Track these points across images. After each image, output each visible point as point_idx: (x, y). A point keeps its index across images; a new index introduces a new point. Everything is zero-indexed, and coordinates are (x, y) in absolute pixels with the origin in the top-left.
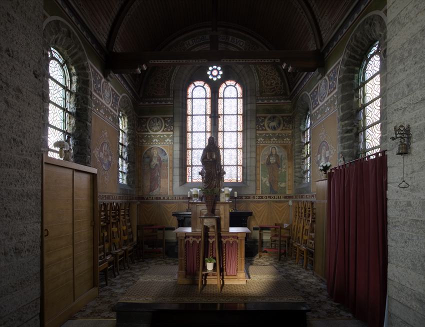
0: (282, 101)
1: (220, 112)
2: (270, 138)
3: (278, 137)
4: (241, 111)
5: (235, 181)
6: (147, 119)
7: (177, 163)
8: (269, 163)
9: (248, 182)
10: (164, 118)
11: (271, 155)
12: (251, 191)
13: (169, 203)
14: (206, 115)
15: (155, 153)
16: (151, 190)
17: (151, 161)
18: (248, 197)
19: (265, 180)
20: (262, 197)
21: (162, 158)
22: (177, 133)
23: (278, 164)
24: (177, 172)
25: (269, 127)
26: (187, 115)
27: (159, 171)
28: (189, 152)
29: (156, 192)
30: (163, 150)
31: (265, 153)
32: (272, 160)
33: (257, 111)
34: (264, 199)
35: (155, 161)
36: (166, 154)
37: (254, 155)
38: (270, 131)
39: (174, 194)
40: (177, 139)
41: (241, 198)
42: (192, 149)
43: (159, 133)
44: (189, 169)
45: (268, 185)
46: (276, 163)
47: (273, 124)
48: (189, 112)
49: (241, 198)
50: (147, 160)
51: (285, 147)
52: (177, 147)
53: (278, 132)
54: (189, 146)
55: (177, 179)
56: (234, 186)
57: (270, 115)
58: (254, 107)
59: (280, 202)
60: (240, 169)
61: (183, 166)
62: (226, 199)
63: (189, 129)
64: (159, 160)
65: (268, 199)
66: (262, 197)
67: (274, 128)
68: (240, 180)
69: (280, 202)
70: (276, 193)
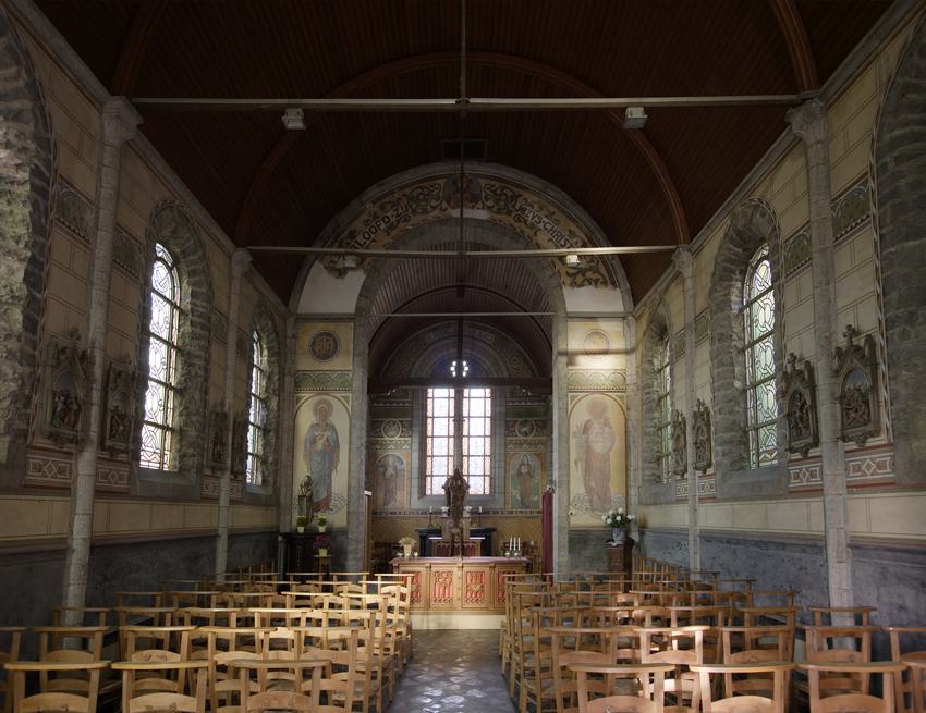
0: (536, 403)
1: (465, 414)
2: (521, 444)
3: (530, 444)
4: (489, 414)
5: (481, 493)
6: (382, 422)
7: (415, 473)
8: (520, 474)
9: (496, 496)
10: (401, 422)
11: (523, 464)
12: (499, 505)
13: (406, 519)
14: (449, 417)
15: (391, 461)
16: (385, 504)
17: (386, 470)
18: (496, 512)
19: (515, 493)
20: (512, 513)
21: (399, 466)
22: (416, 439)
23: (530, 475)
24: (415, 483)
25: (520, 432)
26: (426, 417)
27: (395, 482)
28: (429, 460)
29: (390, 507)
30: (399, 458)
31: (514, 463)
32: (524, 470)
33: (507, 414)
34: (515, 514)
35: (390, 471)
36: (402, 463)
37: (503, 464)
38: (521, 437)
39: (413, 507)
40: (416, 446)
41: (488, 513)
42: (432, 456)
43: (396, 438)
44: (429, 479)
45: (519, 498)
46: (529, 473)
47: (525, 429)
48: (429, 414)
49: (488, 513)
50: (381, 469)
51: (538, 455)
52: (416, 455)
53: (529, 438)
54: (429, 453)
55: (415, 491)
56: (479, 499)
57: (522, 419)
58: (503, 410)
59: (532, 518)
60: (487, 479)
61: (423, 476)
62: (468, 515)
63: (429, 434)
64: (395, 468)
65: (520, 515)
66: (512, 513)
67: (526, 434)
68: (487, 492)
69: (532, 518)
70: (528, 507)
